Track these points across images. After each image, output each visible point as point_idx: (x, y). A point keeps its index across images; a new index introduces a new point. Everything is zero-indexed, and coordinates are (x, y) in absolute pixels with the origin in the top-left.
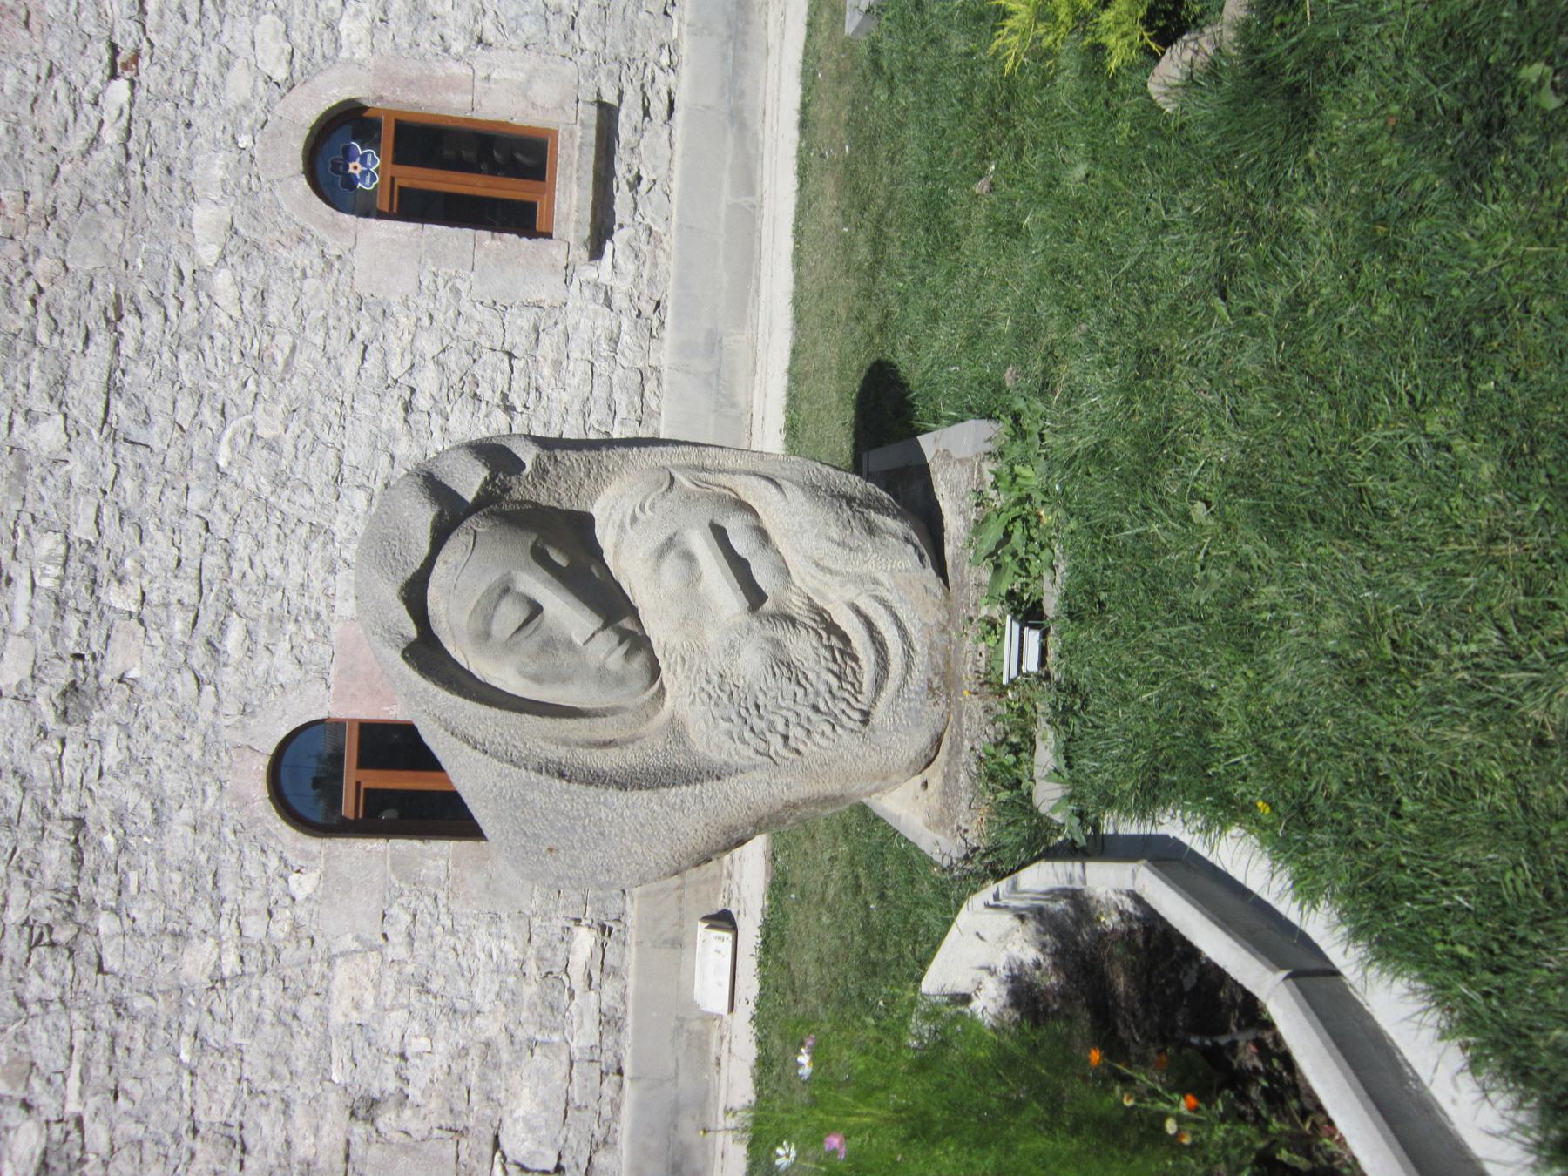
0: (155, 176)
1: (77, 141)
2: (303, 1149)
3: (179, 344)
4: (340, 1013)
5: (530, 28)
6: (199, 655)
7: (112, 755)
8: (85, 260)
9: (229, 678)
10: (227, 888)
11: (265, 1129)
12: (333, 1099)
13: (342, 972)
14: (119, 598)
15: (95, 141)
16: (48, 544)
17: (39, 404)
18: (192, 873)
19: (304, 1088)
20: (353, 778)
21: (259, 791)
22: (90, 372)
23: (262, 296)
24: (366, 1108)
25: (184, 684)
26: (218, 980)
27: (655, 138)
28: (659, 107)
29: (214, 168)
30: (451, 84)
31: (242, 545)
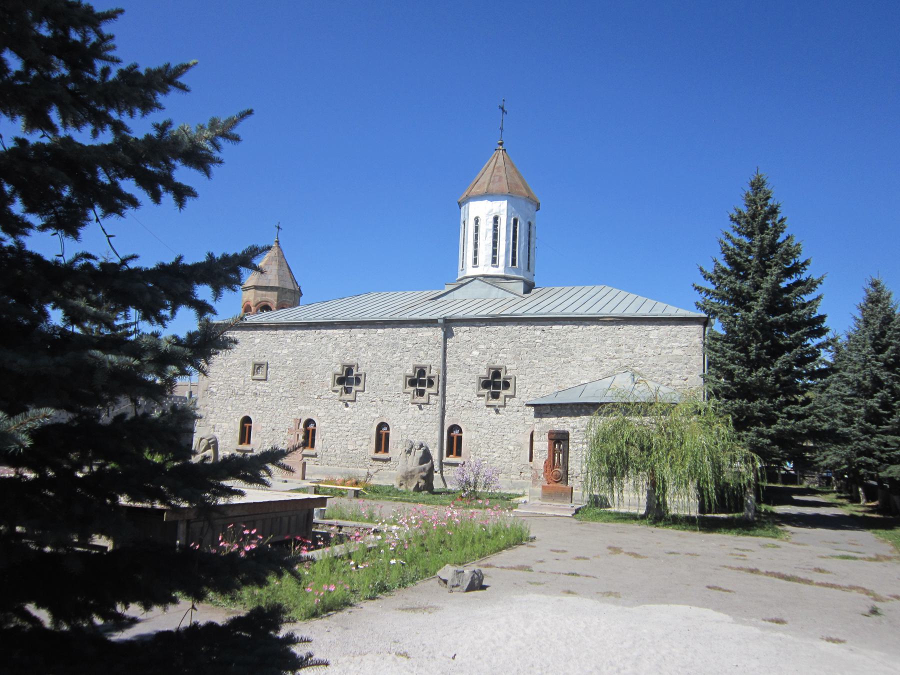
0: (307, 401)
1: (311, 393)
2: (211, 420)
3: (290, 405)
4: (223, 424)
5: (325, 446)
6: (259, 408)
7: (250, 398)
8: (299, 393)
9: (257, 411)
10: (236, 411)
11: (213, 416)
12: (215, 423)
13: (227, 424)
14: (265, 398)
15: (311, 394)
16: (270, 391)
17: (284, 389)
18: (238, 407)
19: (216, 420)
20: (247, 425)
21: (245, 415)
22: (288, 395)
23: (294, 414)
24: (214, 427)
25: (256, 406)
26: (228, 410)
27: (313, 462)
28: (317, 463)
29: (308, 408)
30: (318, 436)
31: (270, 412)
